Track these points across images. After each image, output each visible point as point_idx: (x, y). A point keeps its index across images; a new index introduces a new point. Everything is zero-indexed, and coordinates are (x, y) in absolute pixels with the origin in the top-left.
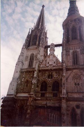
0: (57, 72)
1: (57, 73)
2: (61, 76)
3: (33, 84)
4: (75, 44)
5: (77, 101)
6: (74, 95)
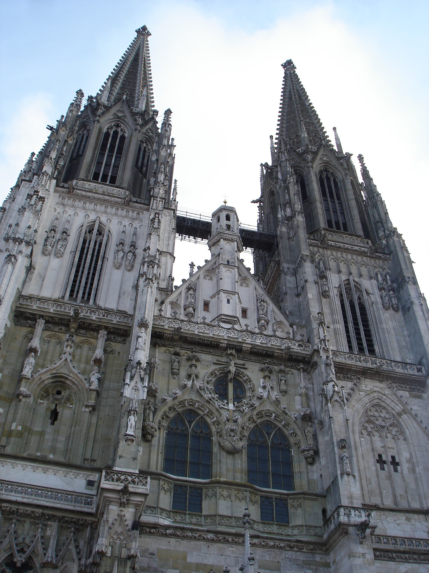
0: (271, 372)
1: (273, 377)
2: (298, 398)
3: (135, 405)
4: (347, 250)
5: (406, 561)
6: (385, 523)
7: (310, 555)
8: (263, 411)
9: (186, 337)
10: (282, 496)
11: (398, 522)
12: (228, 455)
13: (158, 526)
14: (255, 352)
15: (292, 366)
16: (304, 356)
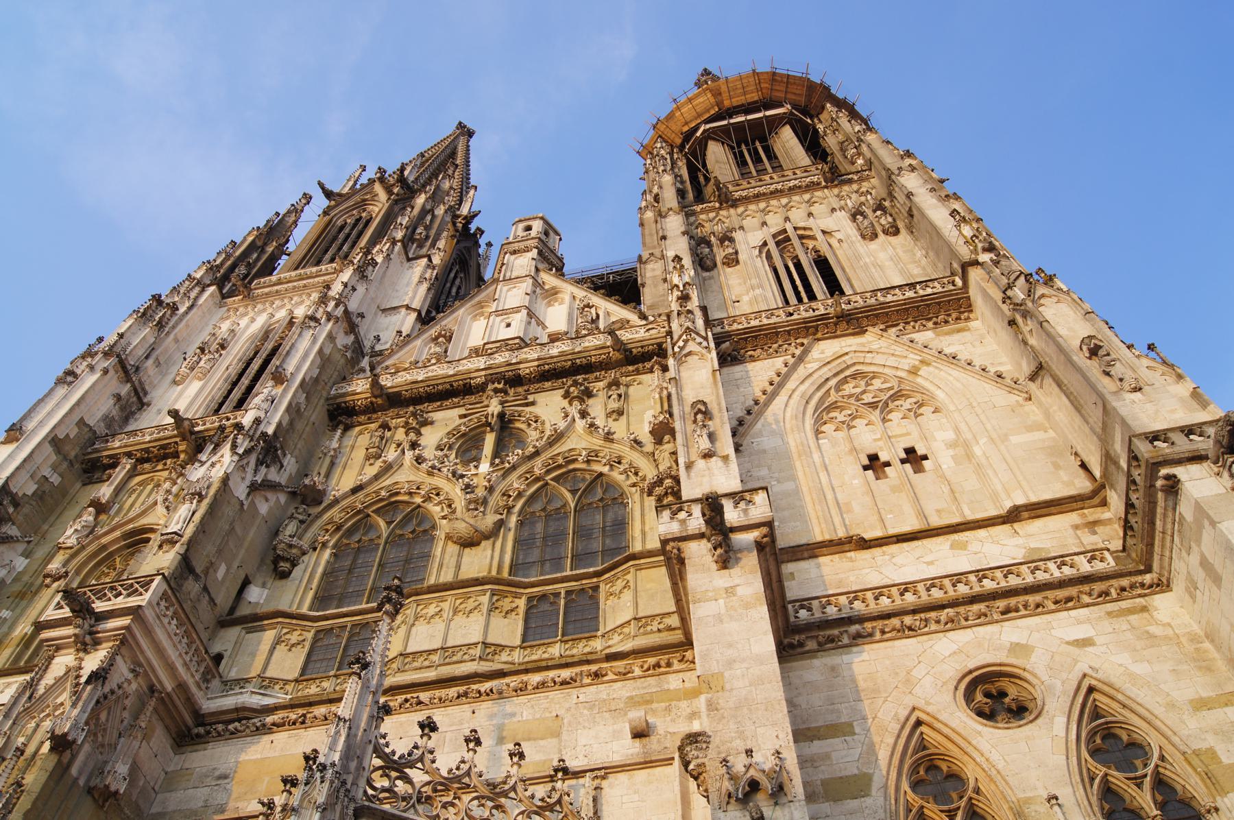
5: (953, 624)
7: (651, 680)
8: (559, 454)
9: (398, 394)
10: (584, 582)
11: (928, 558)
12: (467, 550)
13: (247, 714)
14: (548, 371)
15: (637, 370)
16: (659, 341)
